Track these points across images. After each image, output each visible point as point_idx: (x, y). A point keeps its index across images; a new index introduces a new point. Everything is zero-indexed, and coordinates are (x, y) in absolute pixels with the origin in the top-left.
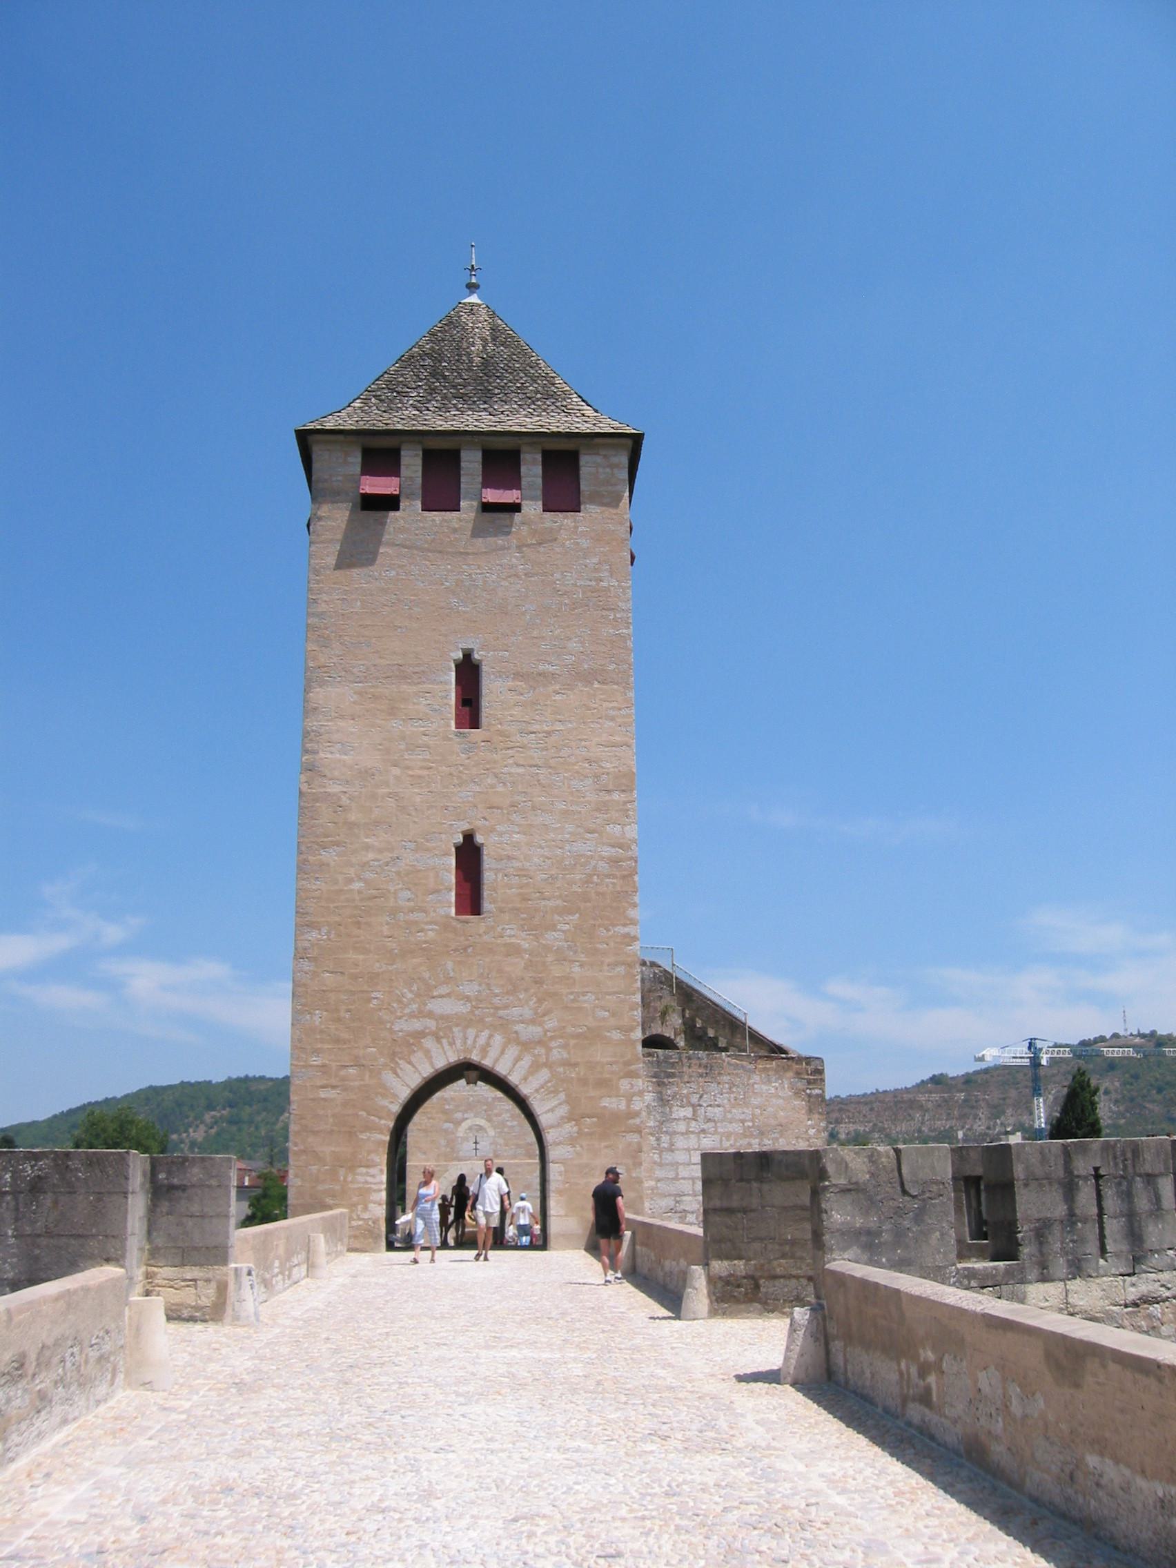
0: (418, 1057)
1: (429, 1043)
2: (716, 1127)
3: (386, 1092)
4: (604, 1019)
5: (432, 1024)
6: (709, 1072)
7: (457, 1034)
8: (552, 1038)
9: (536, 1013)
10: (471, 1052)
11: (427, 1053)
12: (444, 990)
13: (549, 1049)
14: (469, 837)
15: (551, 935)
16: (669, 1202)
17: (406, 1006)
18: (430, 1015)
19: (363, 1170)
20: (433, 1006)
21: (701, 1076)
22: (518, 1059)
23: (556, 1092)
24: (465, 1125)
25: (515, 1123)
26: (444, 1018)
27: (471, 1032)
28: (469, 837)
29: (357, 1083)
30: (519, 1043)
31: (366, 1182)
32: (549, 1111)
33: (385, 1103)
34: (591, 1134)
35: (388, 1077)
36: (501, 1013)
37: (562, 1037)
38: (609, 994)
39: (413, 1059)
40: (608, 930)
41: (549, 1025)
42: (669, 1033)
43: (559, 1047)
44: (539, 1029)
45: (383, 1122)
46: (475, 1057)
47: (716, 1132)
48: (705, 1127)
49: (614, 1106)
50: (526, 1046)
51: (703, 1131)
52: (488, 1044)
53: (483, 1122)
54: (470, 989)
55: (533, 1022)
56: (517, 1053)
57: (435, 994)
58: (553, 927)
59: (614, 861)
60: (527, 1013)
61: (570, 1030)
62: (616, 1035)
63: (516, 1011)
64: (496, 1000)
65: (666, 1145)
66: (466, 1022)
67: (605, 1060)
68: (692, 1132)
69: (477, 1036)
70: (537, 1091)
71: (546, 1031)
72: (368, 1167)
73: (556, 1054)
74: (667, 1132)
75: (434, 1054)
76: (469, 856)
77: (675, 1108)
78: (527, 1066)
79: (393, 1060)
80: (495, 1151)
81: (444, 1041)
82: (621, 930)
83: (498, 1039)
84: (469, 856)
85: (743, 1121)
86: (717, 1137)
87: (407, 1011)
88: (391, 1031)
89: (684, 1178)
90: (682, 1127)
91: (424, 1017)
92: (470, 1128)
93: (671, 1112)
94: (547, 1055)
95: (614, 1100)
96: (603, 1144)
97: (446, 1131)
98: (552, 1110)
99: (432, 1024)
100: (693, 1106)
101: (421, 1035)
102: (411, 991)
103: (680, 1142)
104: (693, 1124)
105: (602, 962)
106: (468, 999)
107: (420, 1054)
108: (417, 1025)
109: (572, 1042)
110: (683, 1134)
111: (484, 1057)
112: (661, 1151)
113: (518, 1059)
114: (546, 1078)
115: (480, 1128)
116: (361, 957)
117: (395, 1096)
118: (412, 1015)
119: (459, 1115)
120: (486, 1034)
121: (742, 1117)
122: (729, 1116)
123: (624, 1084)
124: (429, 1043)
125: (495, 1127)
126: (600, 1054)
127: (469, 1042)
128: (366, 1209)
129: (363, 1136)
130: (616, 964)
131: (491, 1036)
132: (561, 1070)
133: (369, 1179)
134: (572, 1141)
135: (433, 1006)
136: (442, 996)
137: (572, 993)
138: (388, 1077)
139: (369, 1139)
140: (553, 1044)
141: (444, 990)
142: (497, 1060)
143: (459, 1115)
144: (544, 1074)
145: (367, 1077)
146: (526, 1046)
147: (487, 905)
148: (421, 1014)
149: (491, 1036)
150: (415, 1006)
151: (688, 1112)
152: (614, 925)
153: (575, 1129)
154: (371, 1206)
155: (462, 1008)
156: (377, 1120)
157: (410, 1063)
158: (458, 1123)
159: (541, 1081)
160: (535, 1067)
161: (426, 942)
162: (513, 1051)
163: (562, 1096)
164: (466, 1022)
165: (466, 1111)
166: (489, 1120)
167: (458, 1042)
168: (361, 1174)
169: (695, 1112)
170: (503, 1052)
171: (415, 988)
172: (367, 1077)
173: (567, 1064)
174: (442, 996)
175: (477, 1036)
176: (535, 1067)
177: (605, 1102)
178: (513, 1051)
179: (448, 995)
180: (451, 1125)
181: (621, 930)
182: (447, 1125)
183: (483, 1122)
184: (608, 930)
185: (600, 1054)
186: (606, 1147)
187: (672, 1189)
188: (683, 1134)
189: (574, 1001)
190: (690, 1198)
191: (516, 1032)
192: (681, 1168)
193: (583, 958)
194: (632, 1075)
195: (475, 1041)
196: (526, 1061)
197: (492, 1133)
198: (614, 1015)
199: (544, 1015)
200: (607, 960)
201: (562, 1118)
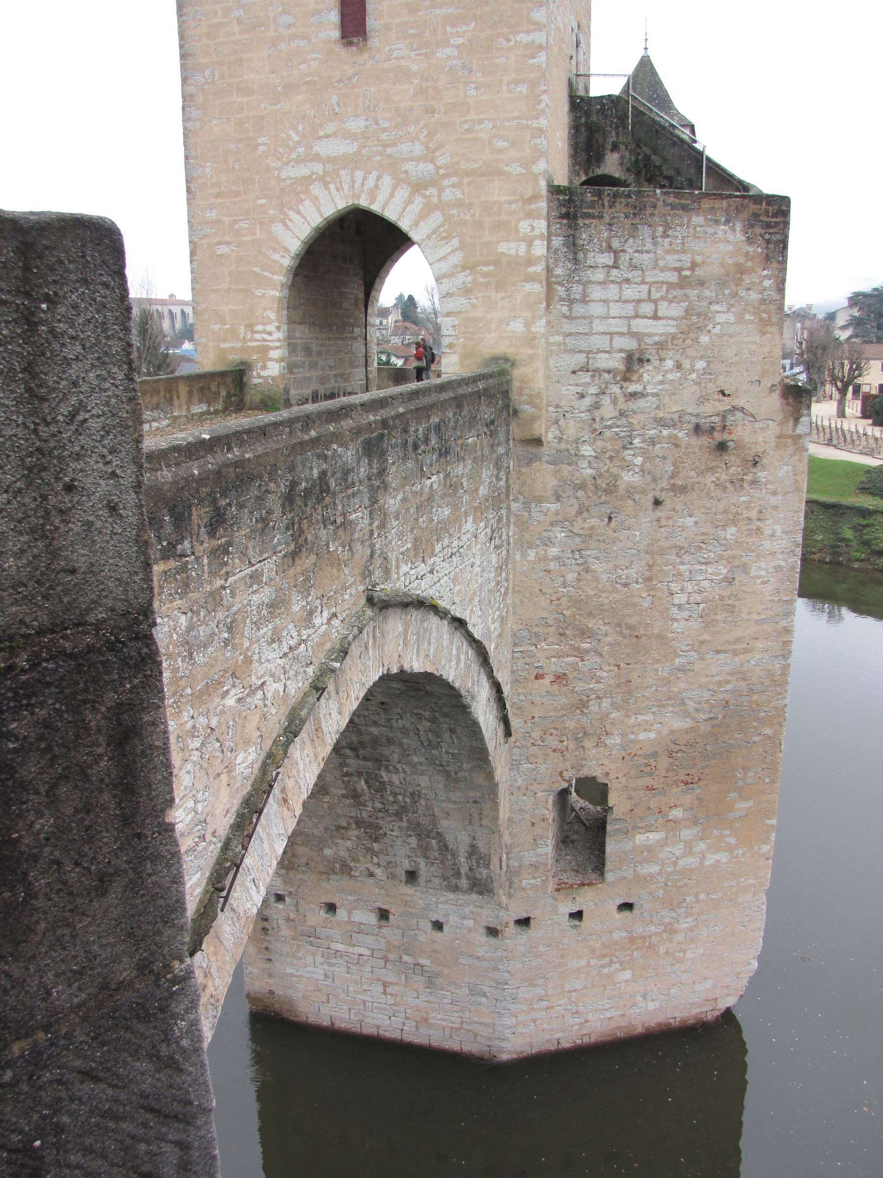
0: (307, 206)
1: (316, 189)
2: (643, 276)
3: (276, 244)
4: (502, 151)
5: (318, 168)
6: (638, 211)
7: (344, 178)
8: (446, 176)
9: (427, 148)
10: (359, 197)
11: (315, 200)
12: (330, 128)
13: (441, 190)
15: (442, 53)
16: (581, 359)
17: (292, 150)
18: (317, 158)
19: (260, 328)
20: (319, 148)
21: (627, 217)
22: (409, 202)
23: (449, 237)
26: (331, 160)
27: (359, 175)
29: (249, 238)
30: (409, 184)
31: (264, 340)
32: (441, 259)
33: (276, 257)
34: (487, 284)
35: (278, 229)
36: (389, 150)
37: (455, 174)
38: (509, 120)
39: (301, 208)
40: (508, 40)
41: (441, 161)
43: (453, 186)
44: (430, 166)
45: (276, 277)
46: (364, 203)
47: (643, 282)
48: (630, 276)
49: (513, 252)
50: (418, 187)
51: (627, 281)
52: (376, 187)
54: (356, 125)
55: (423, 159)
56: (407, 194)
57: (321, 134)
58: (445, 43)
60: (418, 149)
61: (463, 165)
62: (516, 170)
63: (405, 148)
64: (384, 136)
65: (578, 297)
66: (352, 162)
67: (503, 199)
68: (613, 282)
69: (365, 179)
70: (429, 237)
71: (438, 168)
72: (264, 324)
73: (449, 195)
74: (579, 282)
75: (322, 201)
77: (591, 255)
78: (417, 210)
79: (282, 211)
81: (332, 187)
82: (524, 38)
83: (387, 181)
85: (679, 270)
86: (645, 288)
87: (294, 156)
88: (279, 180)
89: (597, 333)
90: (599, 275)
91: (311, 161)
93: (585, 258)
94: (439, 196)
95: (513, 245)
96: (499, 296)
98: (444, 258)
99: (318, 168)
100: (616, 253)
101: (308, 180)
102: (297, 133)
103: (596, 293)
104: (615, 272)
105: (501, 82)
106: (353, 136)
107: (308, 203)
108: (302, 171)
109: (466, 180)
110: (600, 283)
111: (372, 202)
112: (571, 302)
113: (409, 202)
114: (438, 222)
116: (245, 100)
117: (286, 250)
118: (299, 161)
120: (372, 178)
121: (678, 265)
122: (661, 263)
123: (524, 226)
124: (316, 189)
126: (497, 193)
127: (356, 186)
128: (264, 367)
129: (258, 293)
130: (517, 83)
131: (379, 178)
132: (454, 212)
133: (266, 337)
135: (319, 148)
136: (327, 136)
137: (466, 122)
138: (278, 229)
139: (264, 295)
140: (446, 183)
141: (330, 128)
142: (384, 207)
144: (436, 218)
145: (258, 231)
146: (418, 187)
149: (379, 178)
150: (301, 150)
151: (606, 259)
152: (515, 33)
153: (470, 279)
154: (269, 364)
156: (270, 275)
157: (298, 213)
159: (433, 226)
160: (427, 210)
161: (308, 75)
163: (455, 242)
164: (352, 162)
167: (346, 187)
168: (259, 332)
169: (616, 259)
170: (392, 195)
171: (300, 128)
172: (258, 231)
173: (459, 204)
174: (327, 136)
175: (365, 179)
176: (427, 210)
177: (503, 248)
178: (402, 193)
179: (334, 135)
181: (524, 38)
184: (508, 40)
185: (497, 193)
186: (503, 298)
187: (583, 344)
188: (600, 283)
189: (468, 131)
190: (606, 355)
191: (406, 172)
192: (596, 322)
193: (478, 77)
194: (529, 215)
195: (363, 184)
196: (418, 203)
198: (513, 144)
199: (437, 149)
200: (506, 79)
201: (456, 266)
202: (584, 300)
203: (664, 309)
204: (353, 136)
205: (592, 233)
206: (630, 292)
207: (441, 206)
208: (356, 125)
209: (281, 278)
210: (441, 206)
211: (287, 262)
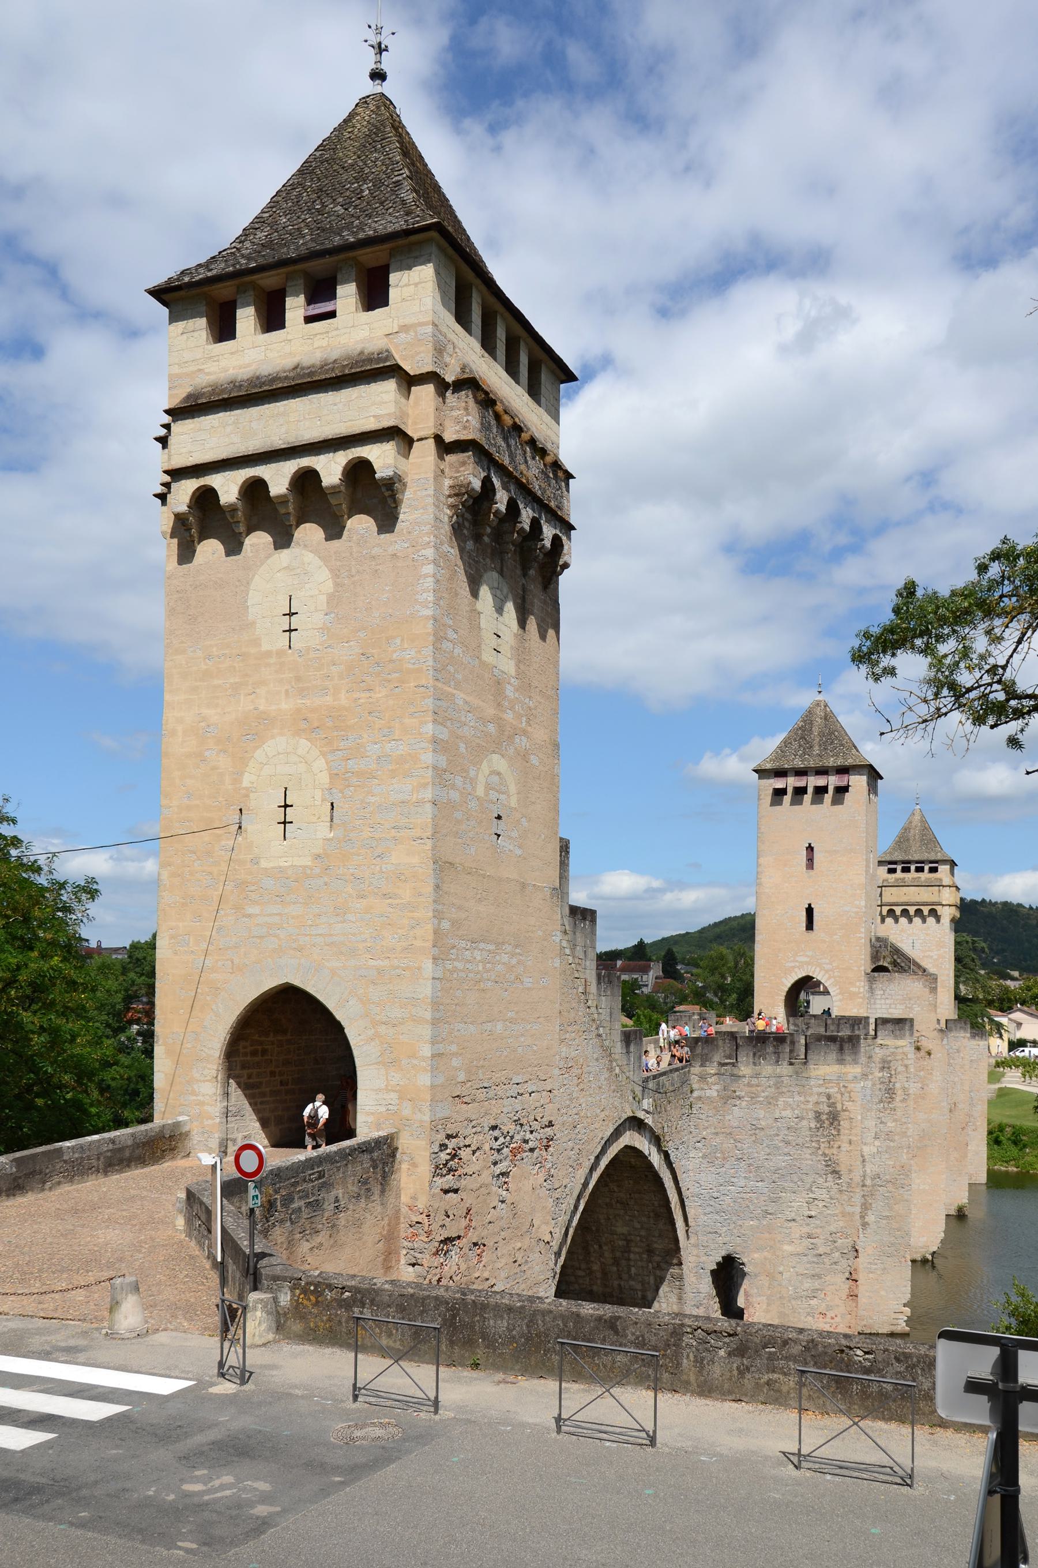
0: (793, 974)
1: (796, 970)
14: (810, 905)
28: (810, 905)
35: (784, 980)
42: (886, 964)
50: (827, 971)
54: (810, 953)
59: (857, 913)
66: (808, 963)
76: (810, 911)
83: (818, 969)
84: (810, 911)
101: (793, 967)
103: (878, 1002)
106: (808, 956)
108: (793, 964)
123: (858, 984)
124: (796, 970)
134: (840, 1000)
138: (784, 980)
146: (827, 971)
147: (815, 927)
148: (795, 961)
155: (806, 959)
160: (829, 978)
162: (823, 972)
164: (808, 963)
176: (829, 978)
178: (823, 972)
196: (827, 976)
202: (875, 1004)
203: (898, 1006)
204: (808, 956)
205: (878, 985)
206: (888, 1001)
207: (834, 977)
208: (810, 953)
209: (785, 994)
210: (834, 977)
211: (787, 989)
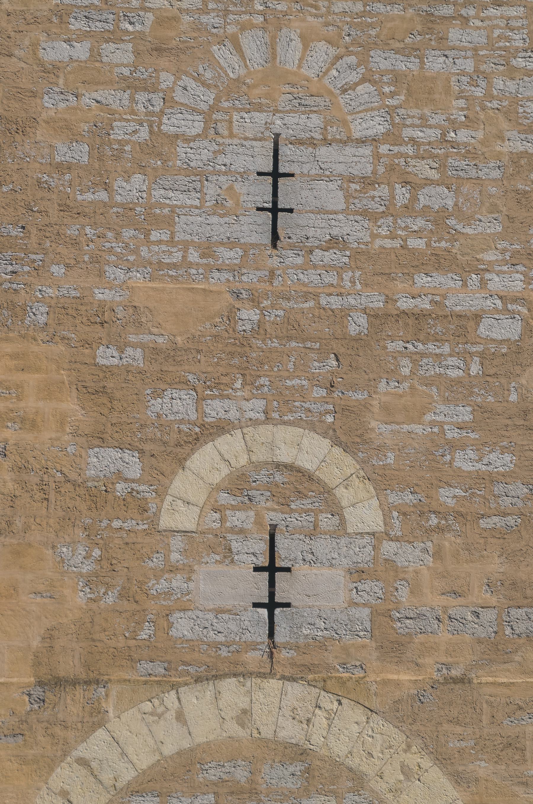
24: (209, 464)
25: (501, 461)
53: (311, 451)
80: (382, 615)
92: (239, 484)
97: (98, 496)
115: (300, 482)
119: (178, 405)
125: (381, 481)
143: (178, 405)
158: (179, 446)
165: (218, 386)
166: (349, 435)
180: (133, 466)
182: (102, 461)
183: (311, 451)
197: (364, 512)
